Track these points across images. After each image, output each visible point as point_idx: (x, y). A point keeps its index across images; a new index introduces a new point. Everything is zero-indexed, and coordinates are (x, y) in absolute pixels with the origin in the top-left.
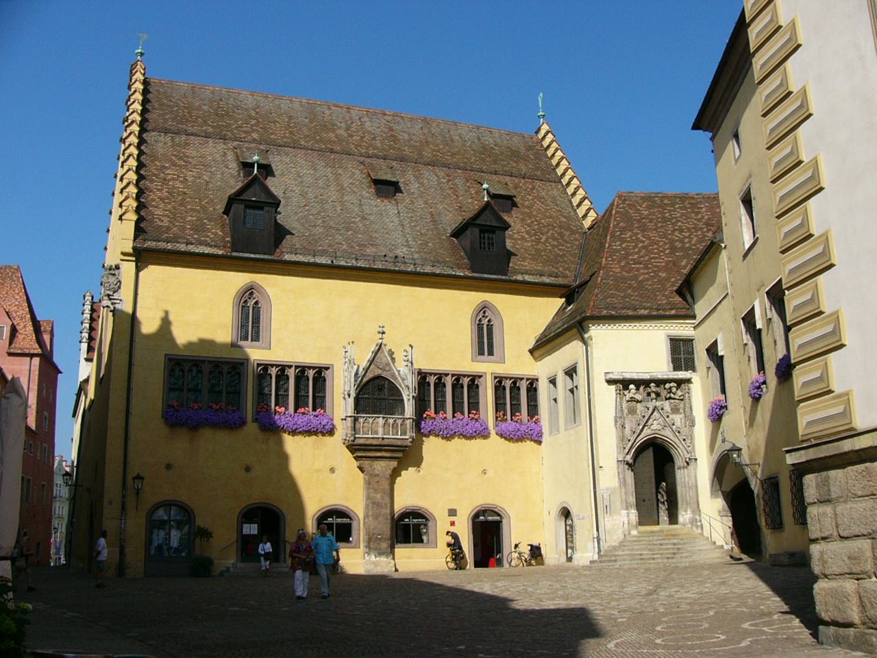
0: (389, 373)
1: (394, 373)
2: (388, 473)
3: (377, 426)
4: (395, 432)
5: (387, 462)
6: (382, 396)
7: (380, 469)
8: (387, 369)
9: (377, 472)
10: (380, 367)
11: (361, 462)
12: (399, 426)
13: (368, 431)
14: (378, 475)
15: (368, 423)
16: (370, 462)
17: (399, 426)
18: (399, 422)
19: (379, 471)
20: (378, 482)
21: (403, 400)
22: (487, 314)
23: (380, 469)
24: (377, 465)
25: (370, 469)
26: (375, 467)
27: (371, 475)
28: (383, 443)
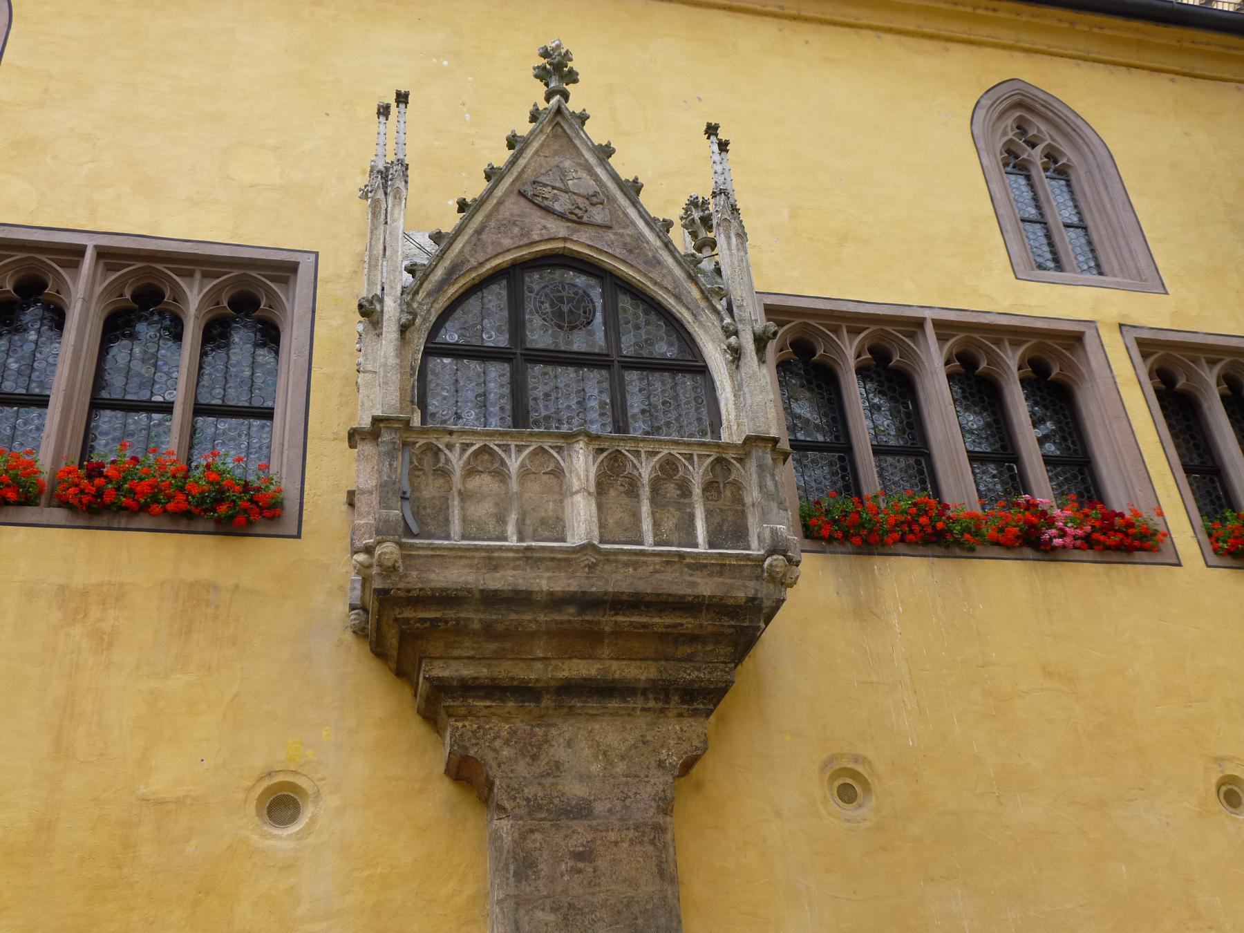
0: (610, 235)
1: (640, 237)
2: (647, 791)
3: (563, 493)
4: (669, 523)
5: (642, 721)
6: (578, 343)
7: (595, 768)
8: (598, 215)
9: (577, 790)
10: (557, 207)
11: (470, 725)
12: (697, 491)
13: (501, 520)
14: (581, 810)
15: (501, 474)
16: (522, 726)
17: (697, 491)
18: (697, 476)
19: (585, 777)
20: (584, 856)
21: (702, 370)
22: (1032, 132)
23: (595, 768)
24: (569, 744)
25: (522, 768)
26: (559, 752)
27: (534, 807)
28: (596, 587)
